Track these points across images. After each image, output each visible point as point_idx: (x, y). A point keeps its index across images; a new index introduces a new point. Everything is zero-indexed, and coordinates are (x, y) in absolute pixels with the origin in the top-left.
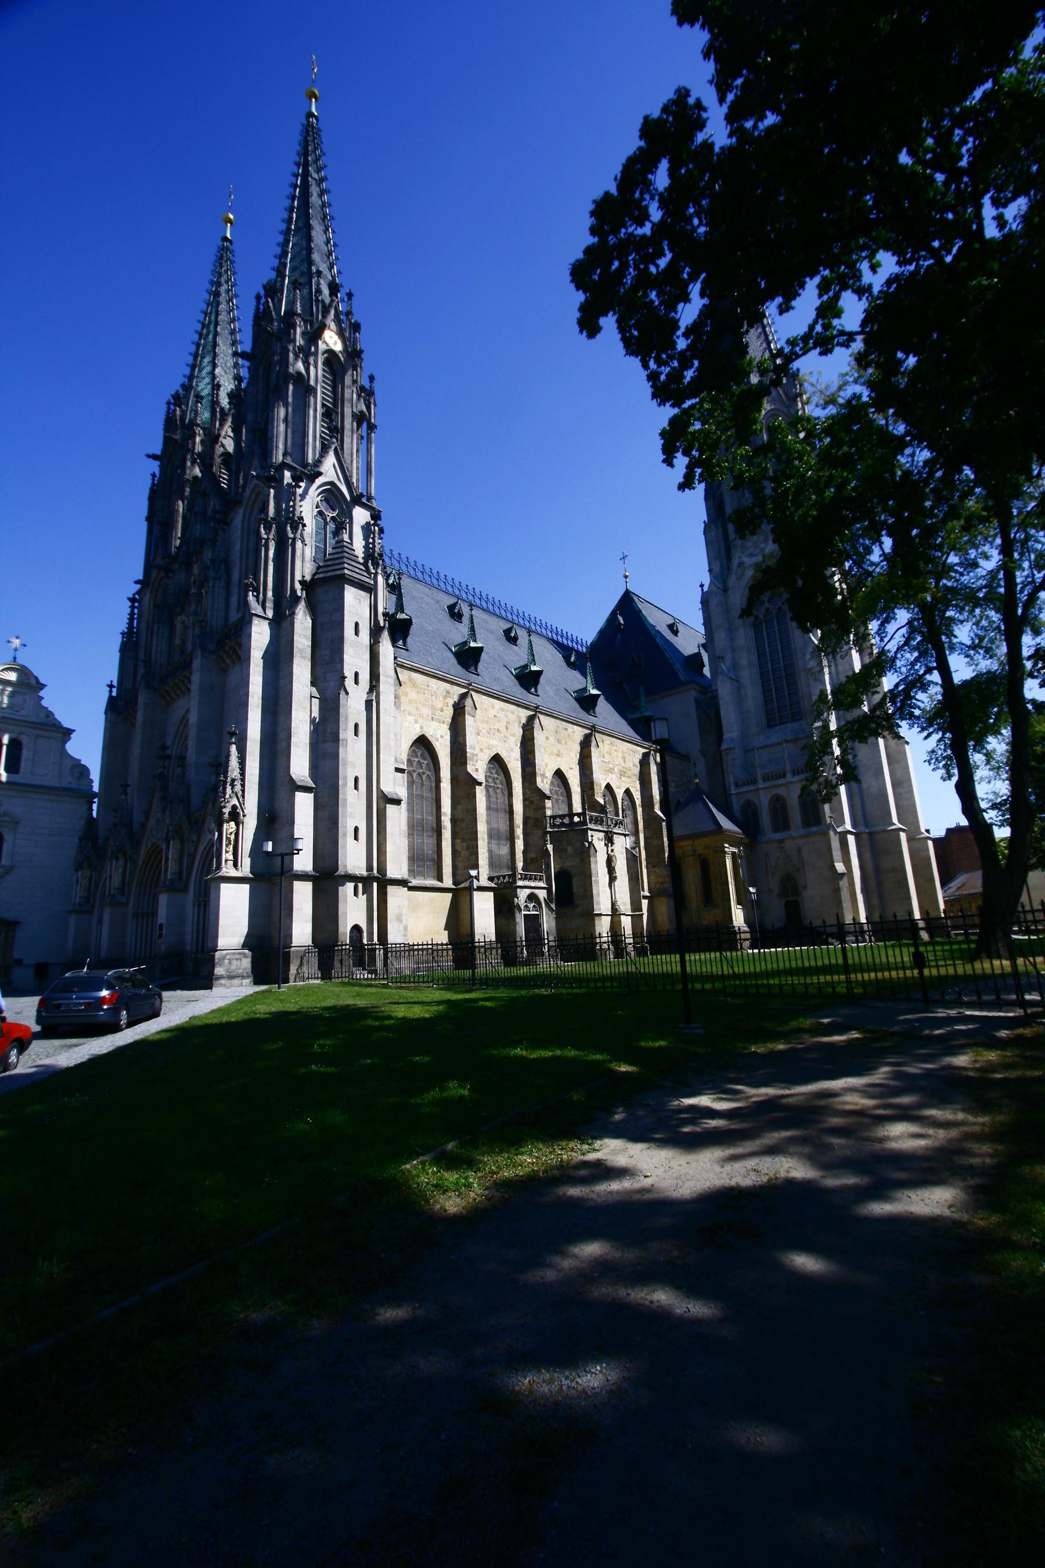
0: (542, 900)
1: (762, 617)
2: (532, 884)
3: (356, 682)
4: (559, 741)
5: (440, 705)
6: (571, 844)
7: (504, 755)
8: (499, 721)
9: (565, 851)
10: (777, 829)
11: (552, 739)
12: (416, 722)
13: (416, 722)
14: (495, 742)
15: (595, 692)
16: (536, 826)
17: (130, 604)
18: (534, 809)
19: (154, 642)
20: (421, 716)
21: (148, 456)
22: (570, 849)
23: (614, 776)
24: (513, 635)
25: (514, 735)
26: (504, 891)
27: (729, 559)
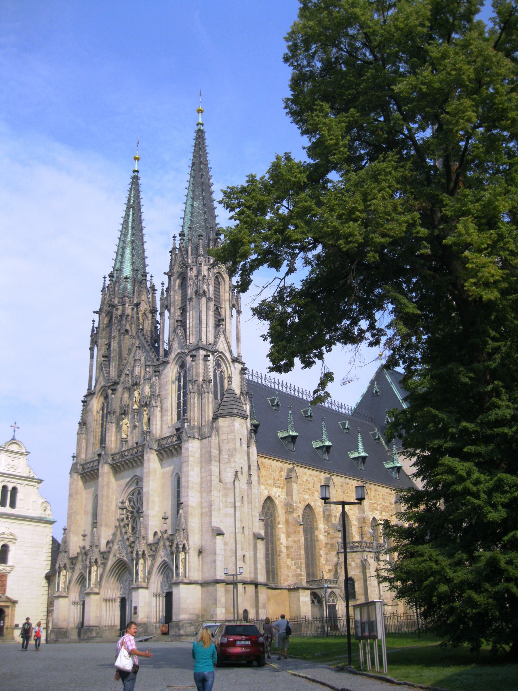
0: (338, 595)
2: (332, 586)
3: (242, 473)
4: (344, 492)
5: (277, 477)
6: (354, 561)
7: (312, 504)
11: (339, 491)
12: (266, 488)
13: (266, 488)
14: (307, 497)
15: (365, 454)
16: (332, 549)
17: (82, 404)
20: (268, 485)
21: (94, 312)
23: (377, 512)
24: (309, 414)
25: (317, 491)
26: (315, 591)
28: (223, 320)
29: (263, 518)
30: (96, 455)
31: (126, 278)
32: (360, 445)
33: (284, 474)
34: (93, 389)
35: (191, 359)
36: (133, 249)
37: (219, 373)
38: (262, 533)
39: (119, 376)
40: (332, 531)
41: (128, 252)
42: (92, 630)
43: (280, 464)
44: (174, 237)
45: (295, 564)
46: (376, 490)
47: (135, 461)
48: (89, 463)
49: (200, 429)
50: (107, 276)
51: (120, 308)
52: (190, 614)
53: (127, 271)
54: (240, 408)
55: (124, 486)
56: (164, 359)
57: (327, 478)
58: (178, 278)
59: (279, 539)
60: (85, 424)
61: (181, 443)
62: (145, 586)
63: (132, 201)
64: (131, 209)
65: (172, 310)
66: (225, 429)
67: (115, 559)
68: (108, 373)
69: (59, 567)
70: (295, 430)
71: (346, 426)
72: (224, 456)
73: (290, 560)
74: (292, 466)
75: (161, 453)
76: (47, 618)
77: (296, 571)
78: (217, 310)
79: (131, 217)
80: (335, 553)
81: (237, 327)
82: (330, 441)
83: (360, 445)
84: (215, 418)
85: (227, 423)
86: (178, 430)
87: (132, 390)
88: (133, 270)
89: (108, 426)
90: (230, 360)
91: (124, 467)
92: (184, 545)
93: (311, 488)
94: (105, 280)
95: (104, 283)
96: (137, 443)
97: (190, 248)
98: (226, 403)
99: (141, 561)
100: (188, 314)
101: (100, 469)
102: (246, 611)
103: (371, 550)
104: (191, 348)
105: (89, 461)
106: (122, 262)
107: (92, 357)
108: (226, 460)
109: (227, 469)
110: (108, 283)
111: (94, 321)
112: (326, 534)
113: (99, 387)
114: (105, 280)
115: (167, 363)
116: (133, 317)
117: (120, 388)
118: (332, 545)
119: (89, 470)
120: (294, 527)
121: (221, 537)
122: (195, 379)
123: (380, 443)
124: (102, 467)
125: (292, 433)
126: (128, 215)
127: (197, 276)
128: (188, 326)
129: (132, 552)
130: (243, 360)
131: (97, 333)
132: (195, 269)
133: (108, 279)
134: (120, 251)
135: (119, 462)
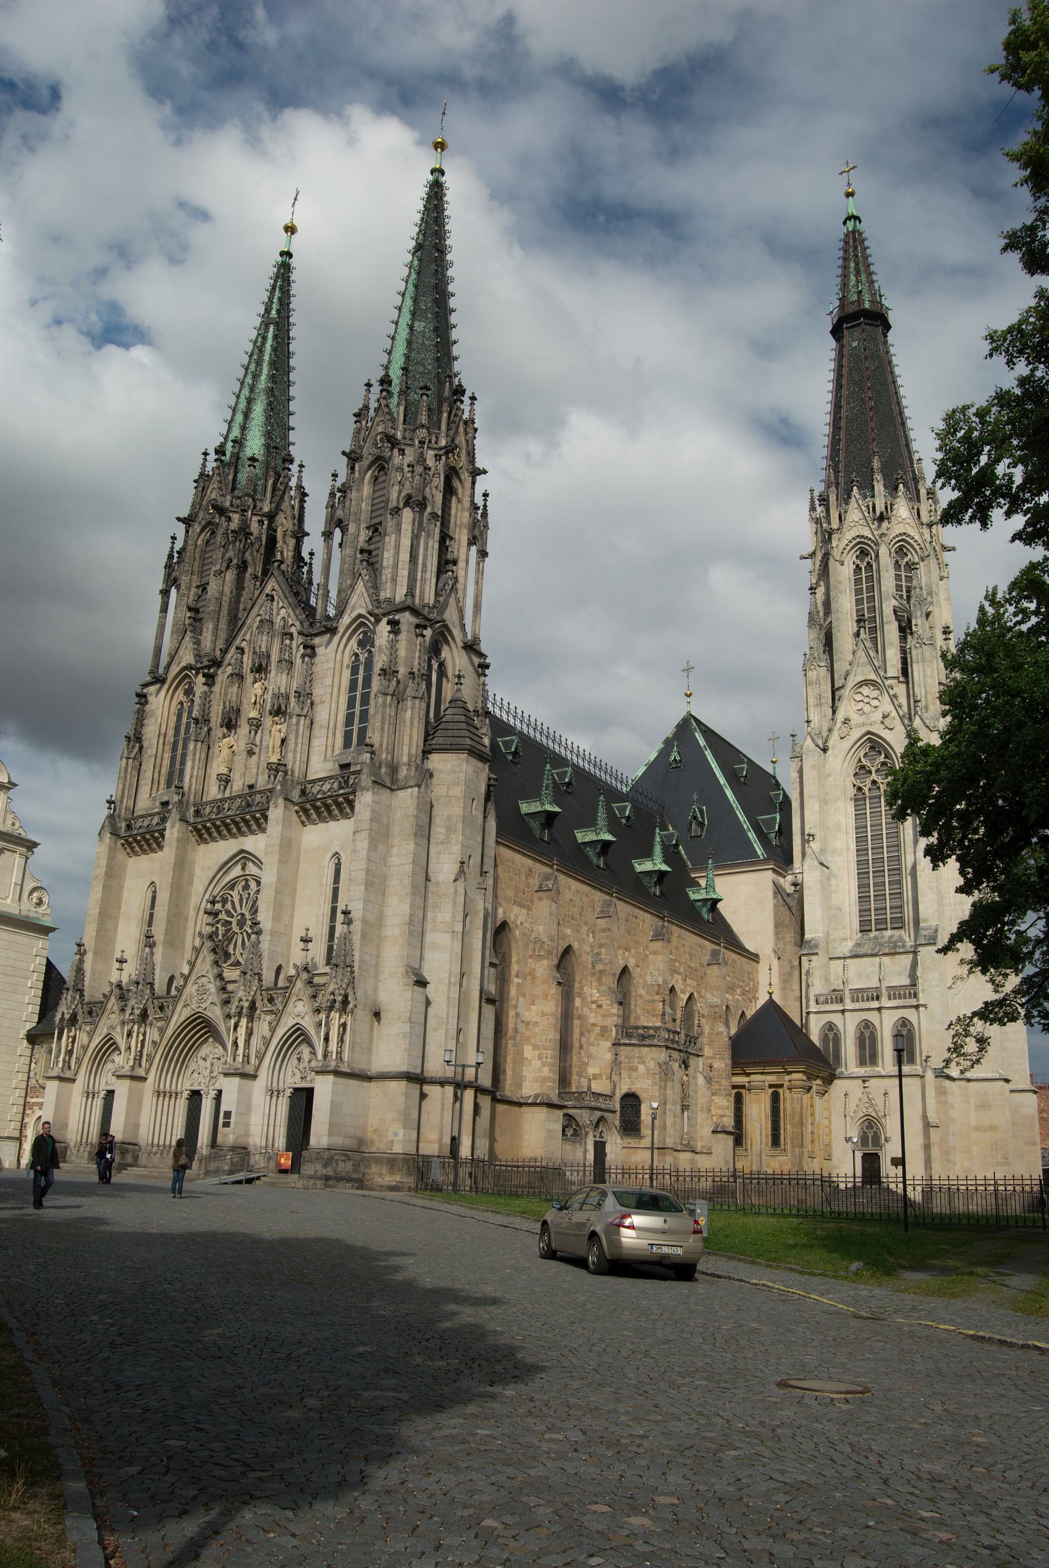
1: (866, 790)
2: (603, 1106)
4: (629, 932)
6: (643, 1063)
7: (576, 945)
8: (574, 906)
9: (636, 1069)
10: (862, 1062)
11: (622, 927)
14: (569, 932)
15: (664, 868)
16: (603, 1036)
18: (602, 1016)
19: (189, 764)
21: (179, 519)
22: (641, 1068)
23: (678, 977)
25: (586, 923)
26: (570, 1111)
27: (834, 712)
28: (455, 562)
29: (495, 961)
30: (158, 803)
31: (253, 459)
32: (658, 849)
33: (535, 883)
34: (161, 671)
35: (389, 628)
36: (270, 404)
37: (435, 666)
38: (492, 988)
39: (225, 652)
40: (606, 1003)
41: (259, 409)
42: (127, 1150)
43: (529, 862)
44: (369, 385)
45: (540, 1058)
46: (680, 936)
47: (246, 822)
48: (142, 817)
49: (394, 769)
50: (212, 452)
51: (236, 518)
52: (347, 1137)
53: (255, 445)
54: (477, 739)
55: (216, 869)
56: (329, 624)
57: (605, 901)
58: (369, 468)
59: (516, 1006)
60: (139, 739)
61: (354, 793)
62: (252, 1073)
63: (274, 312)
64: (272, 328)
65: (352, 528)
66: (443, 776)
67: (187, 1013)
68: (197, 643)
69: (62, 1019)
70: (556, 802)
71: (627, 812)
72: (438, 830)
73: (530, 1048)
74: (550, 871)
75: (306, 811)
76: (23, 1119)
77: (540, 1071)
78: (445, 539)
79: (270, 342)
80: (608, 1044)
81: (477, 583)
82: (610, 831)
83: (658, 849)
84: (426, 753)
85: (449, 765)
86: (344, 767)
87: (249, 678)
88: (267, 446)
89: (191, 746)
90: (460, 644)
91: (219, 832)
92: (346, 996)
93: (577, 916)
94: (205, 460)
95: (204, 465)
96: (251, 787)
97: (402, 408)
98: (450, 726)
99: (244, 1021)
100: (387, 539)
101: (167, 833)
102: (455, 1141)
103: (675, 1046)
104: (389, 608)
105: (141, 813)
106: (244, 428)
107: (164, 609)
108: (441, 836)
109: (442, 856)
110: (211, 464)
111: (174, 538)
112: (594, 1006)
113: (175, 669)
114: (205, 460)
115: (333, 631)
116: (259, 539)
117: (223, 675)
118: (604, 1029)
119: (141, 831)
120: (545, 986)
121: (421, 989)
122: (393, 669)
123: (678, 853)
124: (173, 826)
125: (548, 808)
126: (265, 338)
127: (413, 466)
128: (385, 564)
129: (227, 1002)
130: (484, 648)
131: (178, 563)
132: (408, 451)
133: (212, 456)
134: (242, 405)
135: (209, 820)
